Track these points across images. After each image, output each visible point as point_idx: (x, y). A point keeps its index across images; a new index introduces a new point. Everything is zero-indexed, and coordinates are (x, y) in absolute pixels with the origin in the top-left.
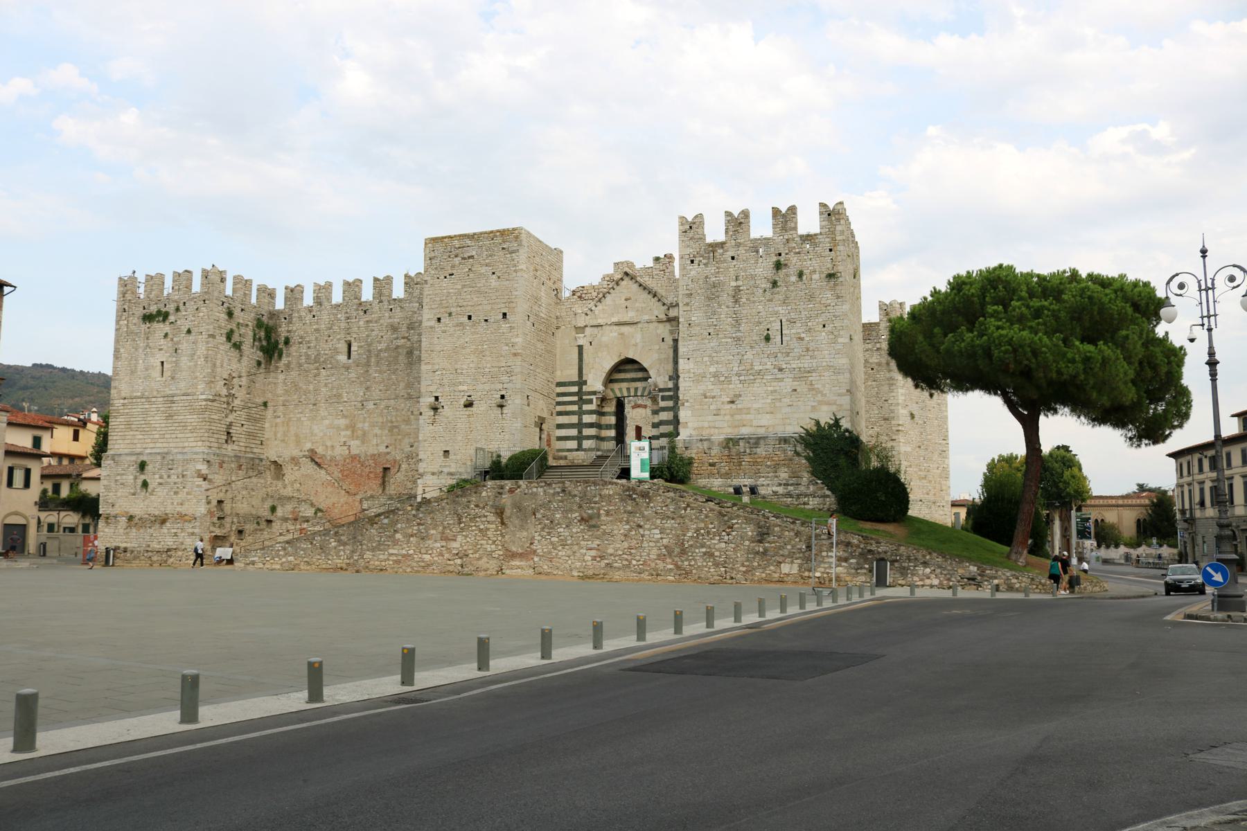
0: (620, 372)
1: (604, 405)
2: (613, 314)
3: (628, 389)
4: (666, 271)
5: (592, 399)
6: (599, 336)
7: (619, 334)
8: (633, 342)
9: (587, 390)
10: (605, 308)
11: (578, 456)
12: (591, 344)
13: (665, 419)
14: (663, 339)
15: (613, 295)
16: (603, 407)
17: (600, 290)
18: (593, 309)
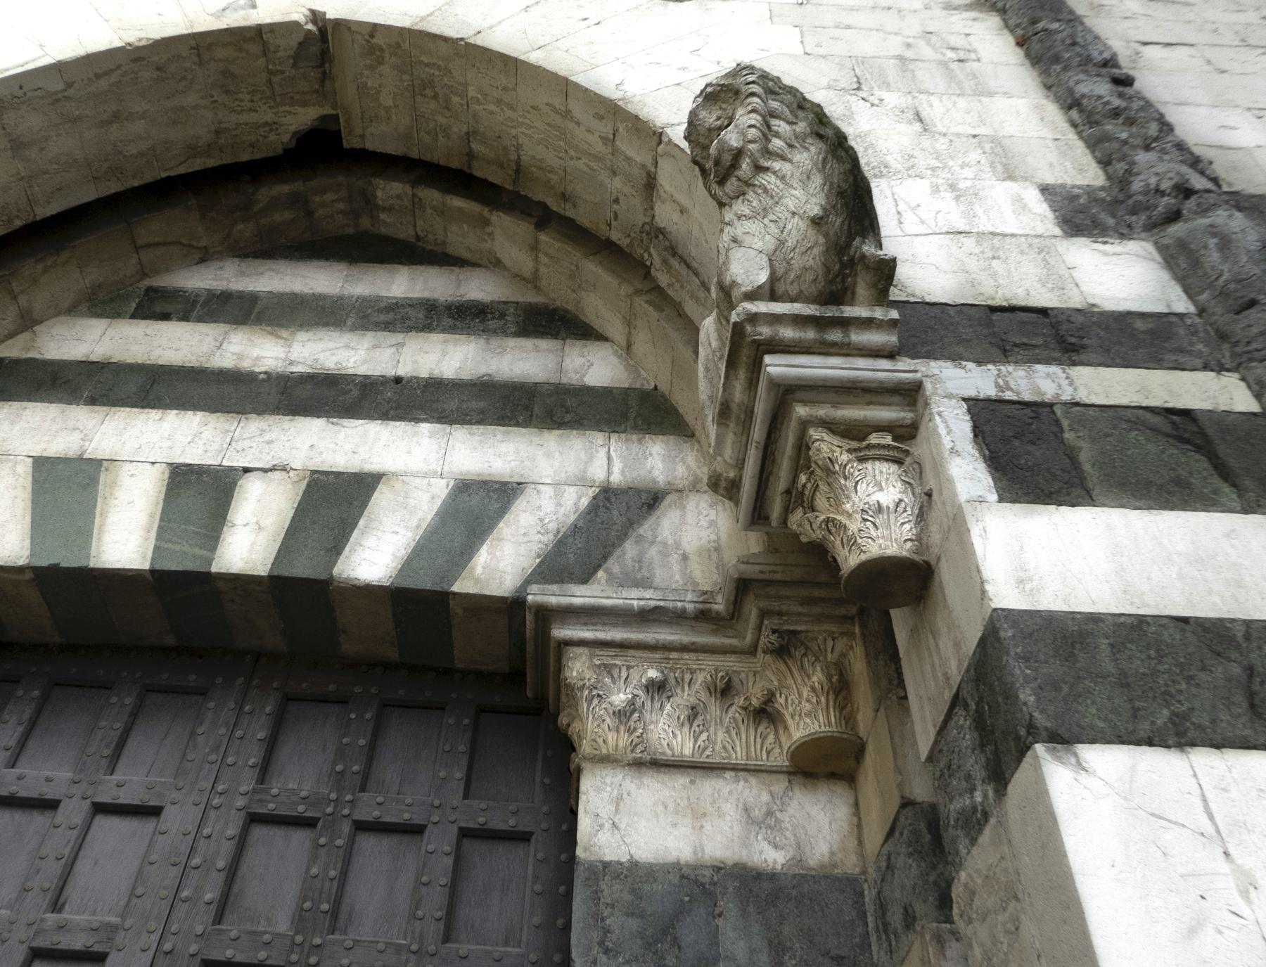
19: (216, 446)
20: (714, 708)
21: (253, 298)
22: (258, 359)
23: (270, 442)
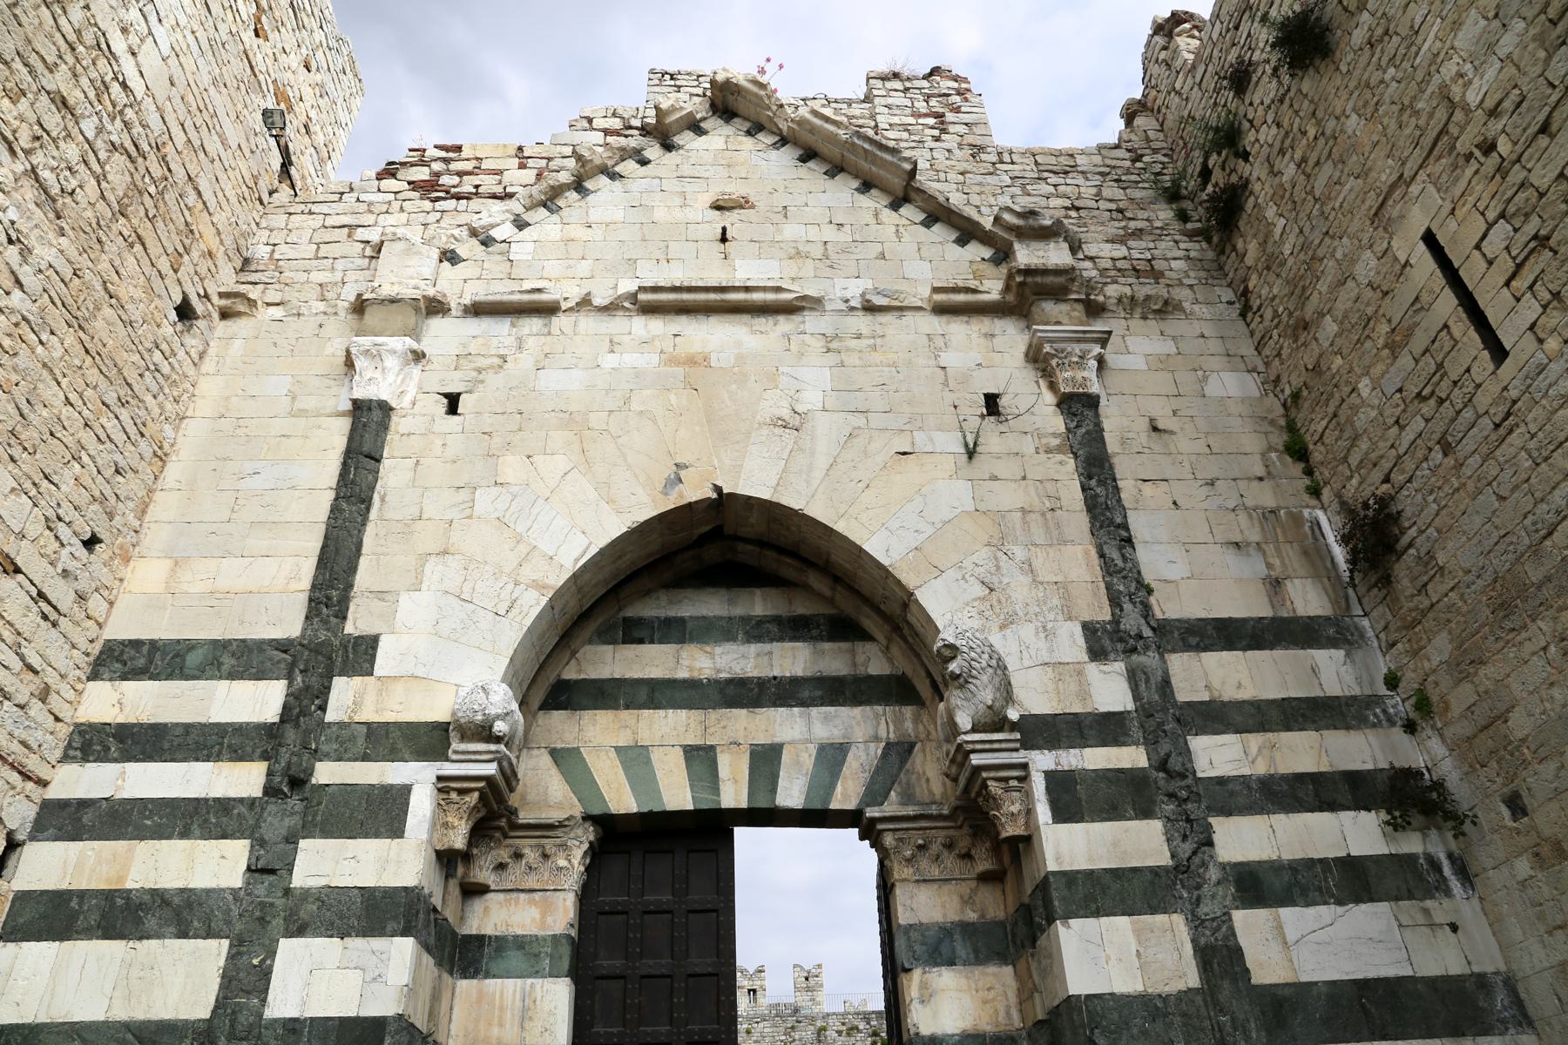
0: (630, 639)
1: (483, 873)
2: (632, 262)
3: (701, 759)
4: (950, 117)
5: (406, 790)
6: (522, 363)
7: (673, 361)
8: (775, 404)
9: (368, 714)
10: (579, 232)
15: (636, 186)
16: (473, 891)
17: (553, 165)
18: (496, 233)
19: (699, 733)
20: (946, 853)
22: (701, 669)
23: (724, 727)
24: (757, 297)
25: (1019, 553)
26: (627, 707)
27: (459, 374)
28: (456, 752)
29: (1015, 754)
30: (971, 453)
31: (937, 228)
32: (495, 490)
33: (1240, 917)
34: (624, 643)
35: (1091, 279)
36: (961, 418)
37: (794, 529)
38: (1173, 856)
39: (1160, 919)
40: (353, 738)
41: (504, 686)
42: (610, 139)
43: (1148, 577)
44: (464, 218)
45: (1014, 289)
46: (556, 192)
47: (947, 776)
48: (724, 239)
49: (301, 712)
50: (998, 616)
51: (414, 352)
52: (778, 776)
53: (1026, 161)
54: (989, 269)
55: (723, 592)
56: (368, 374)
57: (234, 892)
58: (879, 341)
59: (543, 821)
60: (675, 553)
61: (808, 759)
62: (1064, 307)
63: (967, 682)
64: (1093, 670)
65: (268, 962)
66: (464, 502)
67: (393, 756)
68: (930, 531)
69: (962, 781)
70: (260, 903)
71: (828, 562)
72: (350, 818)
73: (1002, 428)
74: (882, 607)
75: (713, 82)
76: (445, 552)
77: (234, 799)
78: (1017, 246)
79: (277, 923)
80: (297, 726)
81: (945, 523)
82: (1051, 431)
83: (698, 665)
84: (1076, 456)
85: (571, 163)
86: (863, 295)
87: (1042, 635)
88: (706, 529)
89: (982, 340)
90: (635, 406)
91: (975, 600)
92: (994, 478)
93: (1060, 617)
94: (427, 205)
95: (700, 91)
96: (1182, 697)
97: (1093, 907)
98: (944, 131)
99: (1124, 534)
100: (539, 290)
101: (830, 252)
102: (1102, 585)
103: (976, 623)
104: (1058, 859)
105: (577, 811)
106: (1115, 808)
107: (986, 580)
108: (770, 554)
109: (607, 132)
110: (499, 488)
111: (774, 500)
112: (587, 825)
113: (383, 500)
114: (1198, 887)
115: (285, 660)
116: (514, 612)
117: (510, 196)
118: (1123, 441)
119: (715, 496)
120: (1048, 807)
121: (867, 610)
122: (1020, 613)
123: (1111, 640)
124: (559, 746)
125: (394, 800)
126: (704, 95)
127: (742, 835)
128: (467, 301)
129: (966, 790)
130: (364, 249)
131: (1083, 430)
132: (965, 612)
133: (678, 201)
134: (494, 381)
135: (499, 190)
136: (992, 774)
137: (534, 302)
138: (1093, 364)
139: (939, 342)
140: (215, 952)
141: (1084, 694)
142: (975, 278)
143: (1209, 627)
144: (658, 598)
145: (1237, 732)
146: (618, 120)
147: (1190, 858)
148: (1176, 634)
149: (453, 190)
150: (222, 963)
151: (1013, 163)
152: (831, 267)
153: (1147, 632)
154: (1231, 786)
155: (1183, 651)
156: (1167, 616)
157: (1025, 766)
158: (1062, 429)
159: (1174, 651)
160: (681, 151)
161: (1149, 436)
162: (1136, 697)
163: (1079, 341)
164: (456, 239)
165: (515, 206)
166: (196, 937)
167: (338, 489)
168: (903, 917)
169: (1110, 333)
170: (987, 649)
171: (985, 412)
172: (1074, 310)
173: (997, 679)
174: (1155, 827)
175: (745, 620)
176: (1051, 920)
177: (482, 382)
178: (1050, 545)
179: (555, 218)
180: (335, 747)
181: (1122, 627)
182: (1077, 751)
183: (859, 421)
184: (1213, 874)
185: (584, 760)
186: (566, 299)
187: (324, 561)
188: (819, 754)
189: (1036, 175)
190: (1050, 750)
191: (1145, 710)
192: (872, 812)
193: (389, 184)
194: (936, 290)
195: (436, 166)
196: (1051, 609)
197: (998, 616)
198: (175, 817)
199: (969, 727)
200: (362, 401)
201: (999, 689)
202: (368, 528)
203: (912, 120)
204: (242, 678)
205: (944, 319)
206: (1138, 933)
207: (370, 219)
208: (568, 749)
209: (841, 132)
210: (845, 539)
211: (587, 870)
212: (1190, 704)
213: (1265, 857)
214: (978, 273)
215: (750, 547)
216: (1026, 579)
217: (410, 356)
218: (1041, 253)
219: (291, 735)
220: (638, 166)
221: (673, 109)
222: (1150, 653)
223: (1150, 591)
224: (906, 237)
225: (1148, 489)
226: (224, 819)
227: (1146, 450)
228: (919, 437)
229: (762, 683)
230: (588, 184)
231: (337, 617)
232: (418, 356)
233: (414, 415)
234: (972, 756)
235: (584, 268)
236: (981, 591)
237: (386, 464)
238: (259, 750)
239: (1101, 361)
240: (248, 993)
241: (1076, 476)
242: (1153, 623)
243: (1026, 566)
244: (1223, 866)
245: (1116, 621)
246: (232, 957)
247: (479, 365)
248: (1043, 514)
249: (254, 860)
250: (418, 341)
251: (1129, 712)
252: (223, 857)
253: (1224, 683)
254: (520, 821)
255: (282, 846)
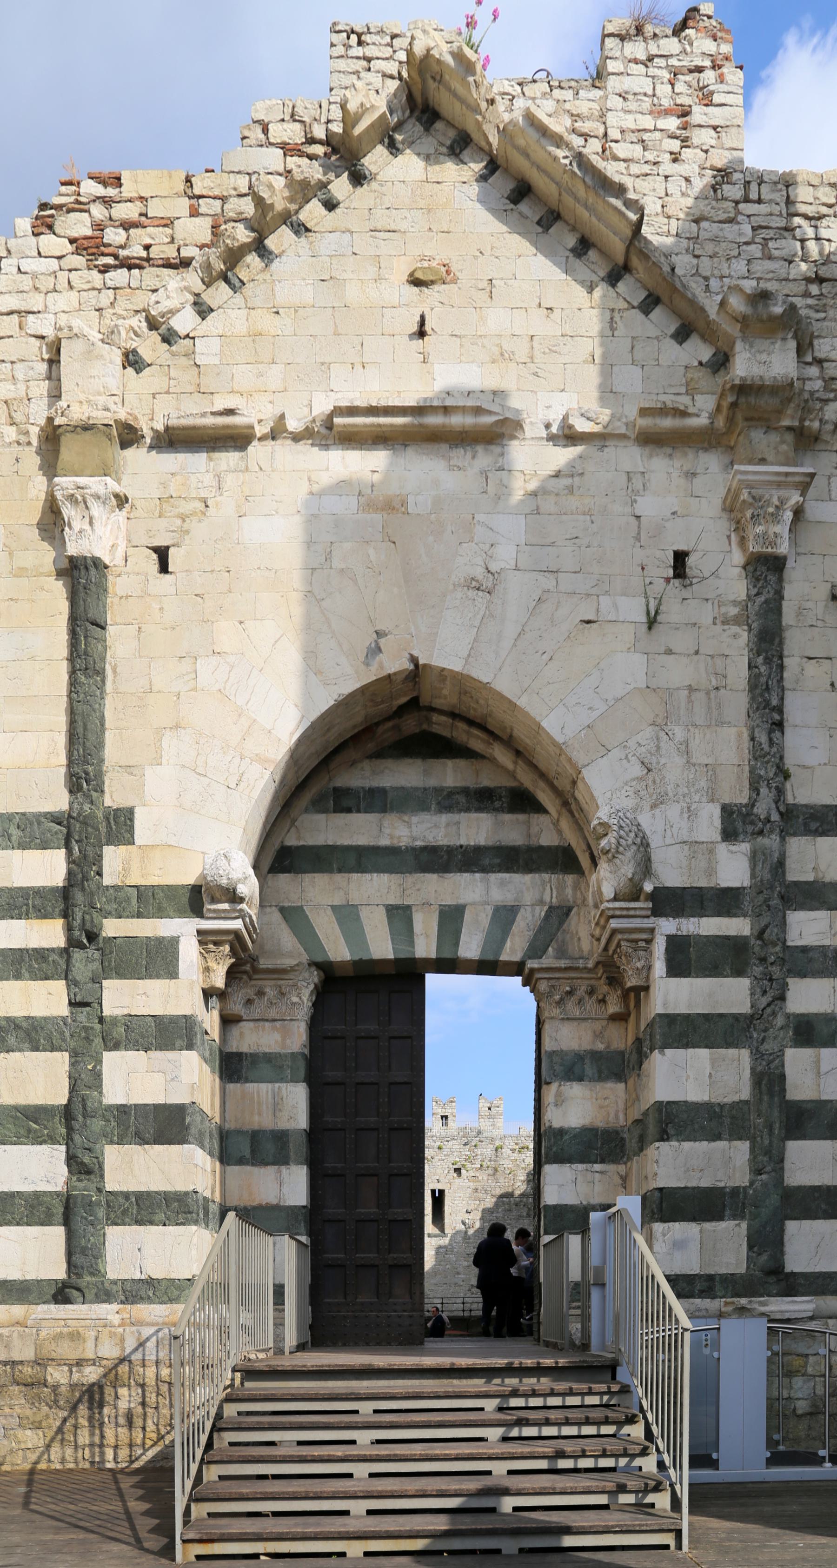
2: (325, 365)
5: (174, 942)
11: (75, 1337)
12: (164, 568)
13: (696, 1093)
14: (680, 558)
15: (326, 243)
21: (382, 792)
22: (399, 837)
24: (456, 421)
25: (679, 733)
26: (340, 871)
27: (163, 523)
28: (209, 910)
29: (646, 920)
30: (652, 623)
31: (657, 313)
32: (214, 660)
33: (791, 1053)
34: (335, 812)
35: (812, 393)
36: (648, 581)
37: (482, 702)
38: (752, 1007)
39: (732, 1052)
40: (128, 900)
41: (241, 853)
42: (293, 162)
43: (790, 762)
44: (142, 299)
45: (725, 410)
46: (234, 257)
47: (593, 936)
48: (421, 333)
49: (83, 877)
50: (651, 796)
51: (117, 496)
52: (460, 932)
53: (777, 197)
54: (703, 379)
55: (419, 762)
56: (77, 525)
57: (64, 1019)
58: (576, 479)
59: (278, 966)
60: (377, 724)
61: (485, 918)
62: (774, 437)
63: (614, 857)
64: (723, 849)
65: (98, 1067)
66: (188, 673)
67: (160, 913)
68: (603, 708)
69: (603, 941)
70: (84, 1027)
71: (511, 736)
72: (136, 963)
73: (686, 593)
74: (555, 782)
75: (410, 53)
76: (177, 727)
77: (48, 950)
78: (739, 346)
79: (98, 1041)
80: (83, 889)
81: (617, 700)
82: (732, 598)
83: (397, 833)
84: (750, 630)
85: (248, 207)
86: (565, 418)
87: (686, 815)
88: (403, 700)
89: (682, 481)
90: (337, 563)
91: (633, 780)
92: (669, 652)
93: (704, 799)
94: (96, 277)
95: (392, 68)
96: (792, 876)
97: (685, 1041)
98: (685, 142)
99: (777, 717)
100: (230, 412)
101: (537, 354)
102: (747, 768)
103: (629, 803)
104: (665, 1004)
105: (305, 958)
106: (716, 967)
107: (646, 761)
108: (462, 726)
109: (287, 149)
110: (217, 658)
111: (465, 672)
112: (313, 969)
113: (114, 671)
114: (765, 1030)
115: (61, 831)
116: (242, 785)
117: (185, 263)
118: (800, 612)
119: (412, 667)
120: (664, 964)
121: (542, 784)
122: (671, 794)
123: (744, 823)
124: (286, 904)
125: (167, 949)
126: (400, 78)
127: (432, 981)
128: (160, 427)
129: (606, 949)
130: (40, 348)
131: (762, 598)
132: (623, 791)
133: (372, 271)
134: (199, 529)
135: (171, 253)
136: (626, 936)
137: (227, 427)
138: (788, 515)
139: (638, 483)
140: (61, 1061)
141: (711, 871)
142: (687, 393)
143: (831, 814)
144: (362, 769)
145: (829, 909)
146: (298, 126)
147: (765, 1008)
148: (801, 818)
149: (123, 253)
150: (67, 1068)
151: (759, 201)
152: (536, 374)
153: (775, 817)
154: (811, 954)
155: (802, 835)
156: (796, 801)
157: (652, 931)
158: (743, 596)
159: (795, 835)
160: (374, 185)
161: (826, 606)
162: (753, 876)
163: (779, 485)
164: (136, 334)
165: (192, 279)
166: (45, 1050)
167: (71, 659)
168: (548, 1045)
169: (812, 476)
170: (634, 828)
171: (671, 572)
172: (783, 442)
173: (639, 856)
174: (745, 983)
175: (438, 790)
176: (652, 1050)
177: (187, 532)
178: (709, 726)
179: (238, 299)
180: (115, 907)
181: (755, 810)
182: (696, 919)
183: (548, 582)
184: (780, 1021)
185: (307, 916)
186: (260, 421)
187: (73, 737)
188: (494, 914)
189: (782, 223)
190: (674, 918)
191: (759, 887)
192: (531, 964)
193: (48, 242)
194: (644, 412)
195: (98, 211)
196: (697, 791)
197: (651, 796)
198: (7, 963)
199: (612, 896)
200: (77, 558)
201: (639, 865)
202: (107, 702)
203: (647, 122)
204: (30, 848)
205: (647, 450)
206: (713, 1061)
207: (35, 302)
208: (294, 907)
209: (560, 153)
210: (526, 714)
211: (315, 1005)
212: (796, 884)
213: (822, 1011)
214: (692, 385)
215: (443, 718)
216: (680, 761)
217: (114, 501)
218: (764, 357)
219: (79, 897)
220: (323, 211)
221: (364, 110)
222: (773, 837)
223: (787, 776)
224: (621, 331)
225: (811, 667)
226: (44, 965)
227: (820, 623)
228: (605, 601)
229: (450, 851)
230: (271, 242)
231: (96, 791)
232: (122, 501)
233: (128, 574)
234: (611, 921)
235: (275, 375)
236: (637, 770)
237: (111, 630)
238: (57, 910)
239: (798, 512)
240: (90, 1088)
241: (746, 652)
242: (782, 809)
243: (683, 747)
244: (788, 1016)
245: (752, 804)
246: (73, 1064)
247: (181, 510)
248: (708, 693)
249: (72, 996)
250: (118, 481)
251: (744, 888)
252: (50, 994)
253: (829, 866)
254: (261, 967)
255: (90, 985)
